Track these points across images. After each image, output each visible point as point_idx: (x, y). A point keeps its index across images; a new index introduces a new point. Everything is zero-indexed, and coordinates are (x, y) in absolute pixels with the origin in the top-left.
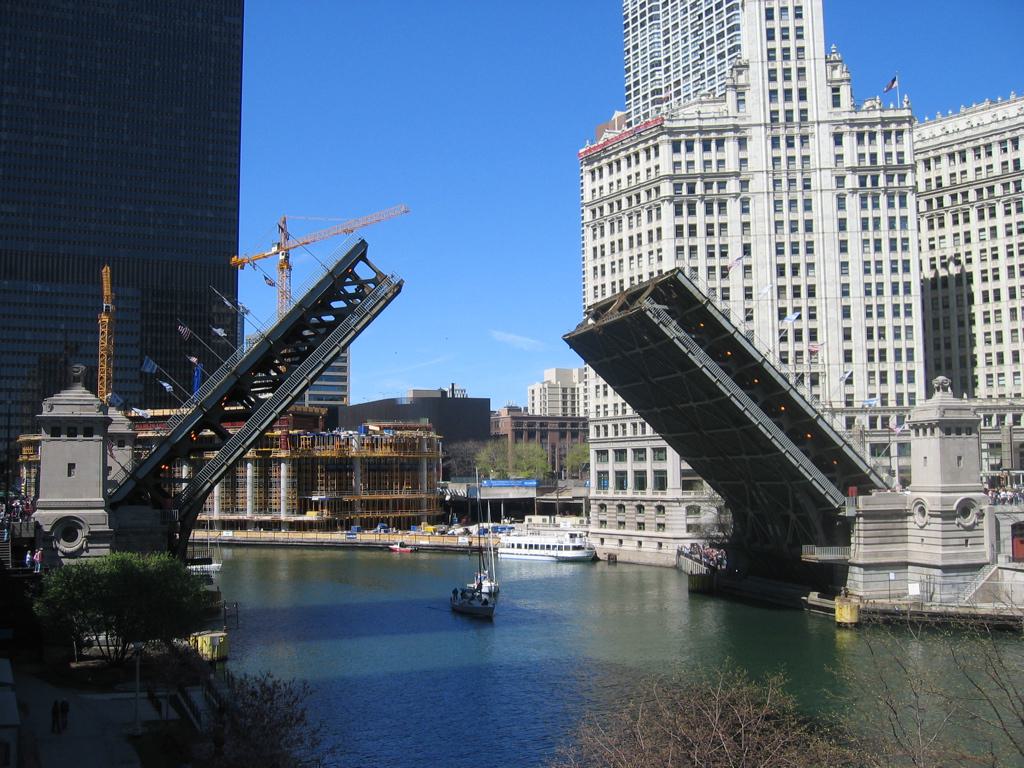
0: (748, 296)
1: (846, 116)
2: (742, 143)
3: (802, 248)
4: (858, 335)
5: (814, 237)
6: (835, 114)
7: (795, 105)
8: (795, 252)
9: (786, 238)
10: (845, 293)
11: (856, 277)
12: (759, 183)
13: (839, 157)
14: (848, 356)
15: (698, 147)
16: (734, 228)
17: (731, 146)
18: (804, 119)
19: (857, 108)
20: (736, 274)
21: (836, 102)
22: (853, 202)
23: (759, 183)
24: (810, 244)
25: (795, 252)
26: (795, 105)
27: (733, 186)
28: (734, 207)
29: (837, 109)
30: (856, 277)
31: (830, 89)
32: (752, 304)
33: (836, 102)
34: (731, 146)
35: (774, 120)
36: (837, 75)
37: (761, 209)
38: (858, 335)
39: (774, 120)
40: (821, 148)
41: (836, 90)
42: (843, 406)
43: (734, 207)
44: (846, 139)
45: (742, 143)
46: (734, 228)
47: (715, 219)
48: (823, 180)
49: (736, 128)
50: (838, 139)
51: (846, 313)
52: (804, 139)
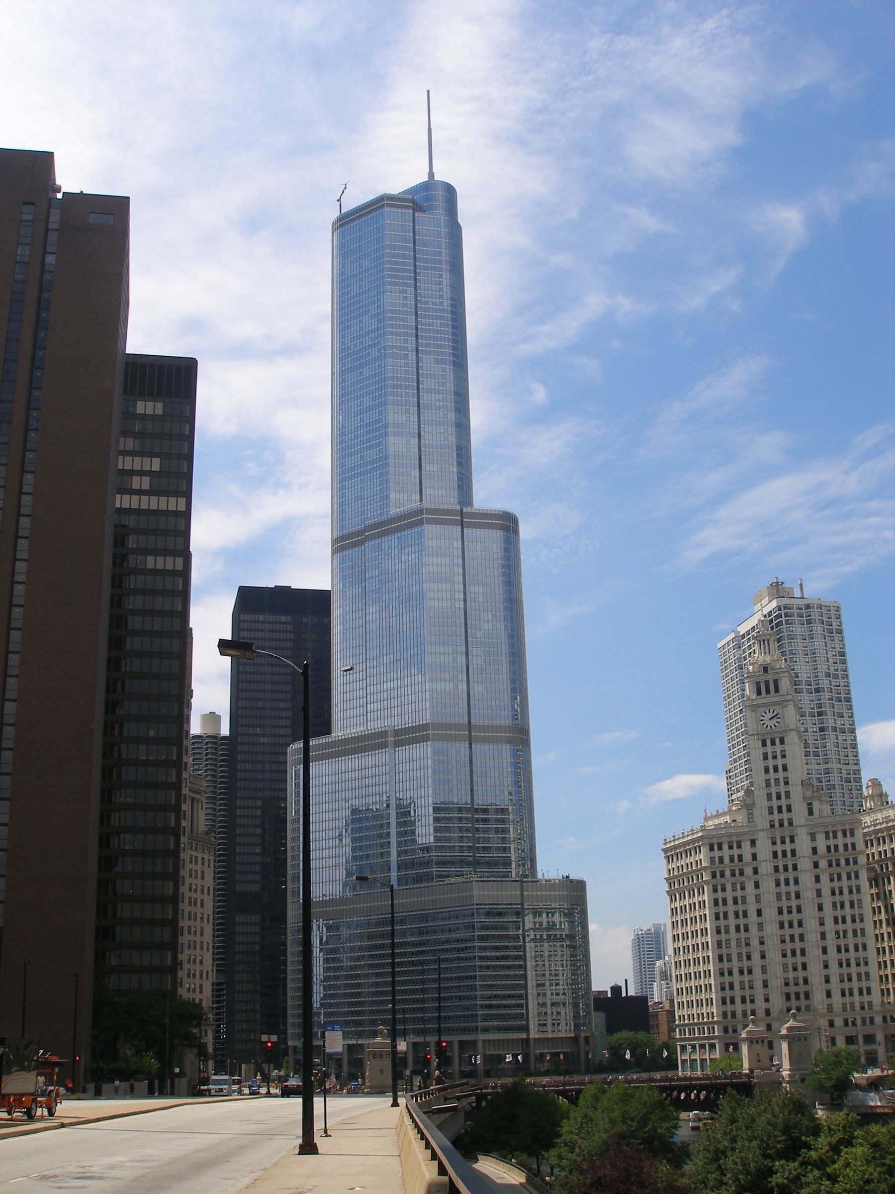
2: (753, 842)
5: (801, 902)
7: (785, 815)
8: (790, 912)
11: (830, 926)
12: (766, 868)
13: (815, 851)
16: (751, 899)
17: (746, 845)
21: (811, 812)
22: (824, 878)
23: (766, 868)
25: (790, 912)
26: (785, 815)
28: (750, 886)
29: (811, 817)
30: (830, 926)
32: (764, 947)
33: (811, 812)
34: (746, 845)
35: (772, 826)
36: (809, 794)
37: (768, 885)
39: (772, 826)
40: (803, 844)
43: (750, 886)
45: (753, 842)
46: (751, 899)
48: (805, 864)
50: (813, 837)
51: (825, 951)
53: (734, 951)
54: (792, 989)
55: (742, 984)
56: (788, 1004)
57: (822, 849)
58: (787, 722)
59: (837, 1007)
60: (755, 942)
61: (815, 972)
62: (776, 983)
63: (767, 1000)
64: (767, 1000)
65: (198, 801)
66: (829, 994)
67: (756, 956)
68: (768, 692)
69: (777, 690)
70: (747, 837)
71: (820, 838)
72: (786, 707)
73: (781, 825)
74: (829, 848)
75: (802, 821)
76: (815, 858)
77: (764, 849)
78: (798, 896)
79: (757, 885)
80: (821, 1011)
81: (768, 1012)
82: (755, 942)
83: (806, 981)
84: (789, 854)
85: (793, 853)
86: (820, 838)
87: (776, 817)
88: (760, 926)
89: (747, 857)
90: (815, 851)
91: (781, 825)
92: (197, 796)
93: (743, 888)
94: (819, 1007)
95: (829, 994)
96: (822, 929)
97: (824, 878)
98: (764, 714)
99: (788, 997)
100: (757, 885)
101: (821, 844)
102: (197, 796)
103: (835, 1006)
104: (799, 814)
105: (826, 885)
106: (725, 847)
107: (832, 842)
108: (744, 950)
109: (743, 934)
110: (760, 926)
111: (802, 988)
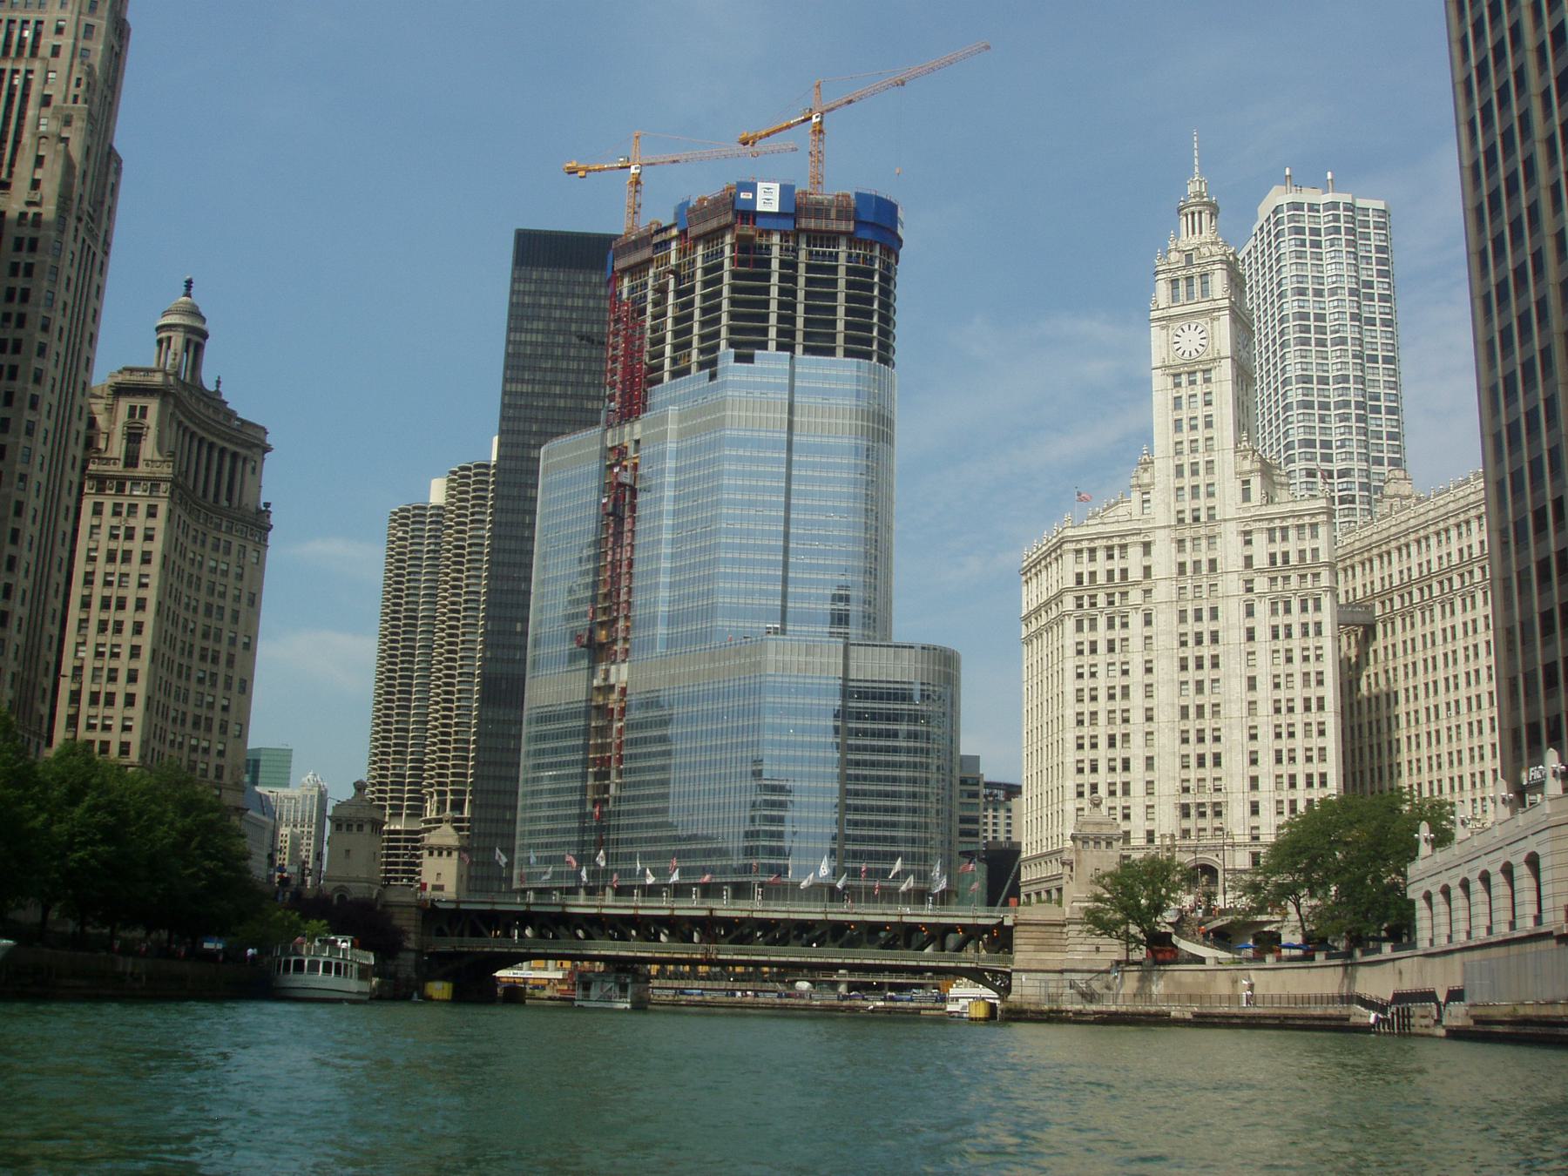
0: (1149, 719)
1: (1253, 512)
2: (1147, 546)
3: (1207, 663)
4: (1266, 759)
6: (1245, 510)
7: (1203, 503)
9: (1191, 652)
13: (1248, 561)
14: (1254, 783)
15: (1101, 555)
16: (1136, 643)
17: (1135, 553)
18: (1211, 517)
19: (1270, 500)
21: (1246, 496)
22: (1262, 608)
23: (1163, 591)
24: (1215, 657)
27: (1135, 596)
28: (1136, 620)
31: (1239, 482)
32: (1153, 727)
33: (1246, 496)
34: (1135, 553)
35: (1181, 521)
38: (1266, 759)
39: (1181, 521)
40: (1230, 551)
41: (1246, 482)
42: (1247, 839)
43: (1136, 620)
44: (1255, 537)
46: (1136, 643)
47: (1117, 634)
48: (1231, 584)
49: (1138, 532)
52: (1211, 539)
54: (1189, 799)
57: (1261, 561)
58: (1217, 346)
60: (1137, 716)
62: (1167, 788)
65: (245, 460)
68: (1190, 295)
69: (1205, 292)
70: (1135, 538)
71: (1260, 539)
72: (1218, 318)
73: (1196, 519)
74: (1273, 556)
75: (1231, 512)
76: (1249, 574)
77: (1164, 558)
78: (1215, 638)
79: (1148, 622)
84: (1205, 568)
85: (1213, 563)
86: (1260, 539)
87: (1187, 505)
89: (1135, 574)
90: (1248, 561)
91: (1196, 519)
92: (243, 451)
93: (1125, 625)
96: (1251, 696)
97: (1262, 608)
98: (1180, 332)
99: (1185, 811)
100: (1148, 622)
101: (1261, 550)
102: (243, 451)
103: (1263, 830)
104: (1228, 501)
105: (1263, 621)
106: (1101, 555)
107: (1278, 548)
109: (1118, 704)
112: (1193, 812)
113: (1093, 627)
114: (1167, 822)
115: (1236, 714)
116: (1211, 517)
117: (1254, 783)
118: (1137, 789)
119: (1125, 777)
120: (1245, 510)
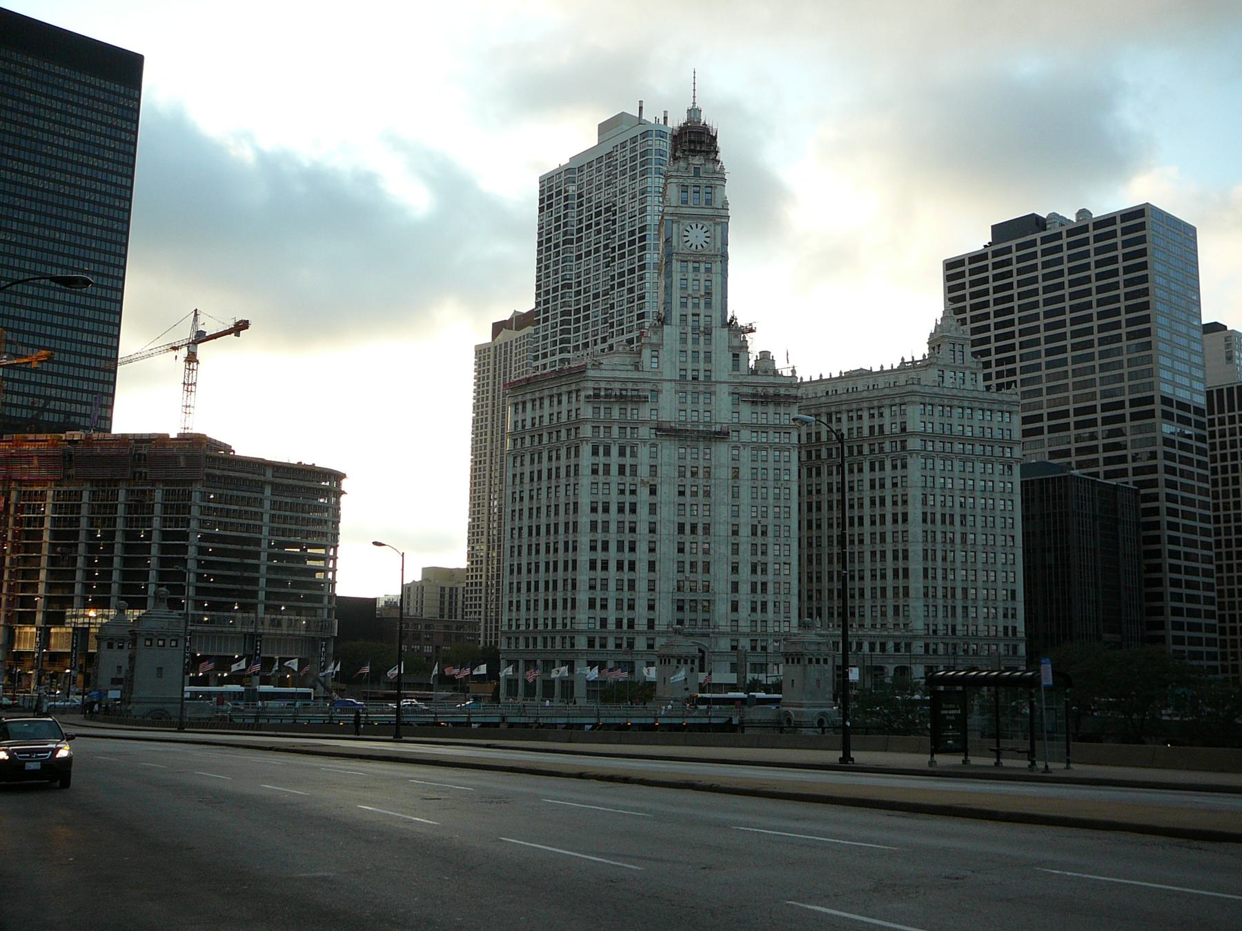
10: (735, 533)
14: (735, 587)
18: (708, 378)
20: (643, 512)
35: (683, 377)
53: (613, 537)
55: (620, 582)
56: (680, 615)
59: (744, 626)
60: (643, 528)
61: (721, 577)
62: (666, 585)
63: (651, 607)
64: (651, 607)
66: (735, 607)
67: (642, 547)
80: (722, 629)
81: (651, 624)
82: (643, 528)
83: (707, 589)
88: (653, 509)
94: (722, 623)
95: (735, 607)
103: (741, 623)
108: (627, 537)
110: (653, 509)
111: (700, 596)
112: (687, 607)
113: (882, 468)
114: (665, 613)
115: (723, 533)
116: (708, 378)
117: (735, 587)
118: (642, 586)
119: (632, 575)
120: (735, 376)
